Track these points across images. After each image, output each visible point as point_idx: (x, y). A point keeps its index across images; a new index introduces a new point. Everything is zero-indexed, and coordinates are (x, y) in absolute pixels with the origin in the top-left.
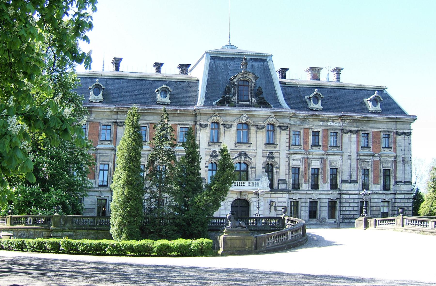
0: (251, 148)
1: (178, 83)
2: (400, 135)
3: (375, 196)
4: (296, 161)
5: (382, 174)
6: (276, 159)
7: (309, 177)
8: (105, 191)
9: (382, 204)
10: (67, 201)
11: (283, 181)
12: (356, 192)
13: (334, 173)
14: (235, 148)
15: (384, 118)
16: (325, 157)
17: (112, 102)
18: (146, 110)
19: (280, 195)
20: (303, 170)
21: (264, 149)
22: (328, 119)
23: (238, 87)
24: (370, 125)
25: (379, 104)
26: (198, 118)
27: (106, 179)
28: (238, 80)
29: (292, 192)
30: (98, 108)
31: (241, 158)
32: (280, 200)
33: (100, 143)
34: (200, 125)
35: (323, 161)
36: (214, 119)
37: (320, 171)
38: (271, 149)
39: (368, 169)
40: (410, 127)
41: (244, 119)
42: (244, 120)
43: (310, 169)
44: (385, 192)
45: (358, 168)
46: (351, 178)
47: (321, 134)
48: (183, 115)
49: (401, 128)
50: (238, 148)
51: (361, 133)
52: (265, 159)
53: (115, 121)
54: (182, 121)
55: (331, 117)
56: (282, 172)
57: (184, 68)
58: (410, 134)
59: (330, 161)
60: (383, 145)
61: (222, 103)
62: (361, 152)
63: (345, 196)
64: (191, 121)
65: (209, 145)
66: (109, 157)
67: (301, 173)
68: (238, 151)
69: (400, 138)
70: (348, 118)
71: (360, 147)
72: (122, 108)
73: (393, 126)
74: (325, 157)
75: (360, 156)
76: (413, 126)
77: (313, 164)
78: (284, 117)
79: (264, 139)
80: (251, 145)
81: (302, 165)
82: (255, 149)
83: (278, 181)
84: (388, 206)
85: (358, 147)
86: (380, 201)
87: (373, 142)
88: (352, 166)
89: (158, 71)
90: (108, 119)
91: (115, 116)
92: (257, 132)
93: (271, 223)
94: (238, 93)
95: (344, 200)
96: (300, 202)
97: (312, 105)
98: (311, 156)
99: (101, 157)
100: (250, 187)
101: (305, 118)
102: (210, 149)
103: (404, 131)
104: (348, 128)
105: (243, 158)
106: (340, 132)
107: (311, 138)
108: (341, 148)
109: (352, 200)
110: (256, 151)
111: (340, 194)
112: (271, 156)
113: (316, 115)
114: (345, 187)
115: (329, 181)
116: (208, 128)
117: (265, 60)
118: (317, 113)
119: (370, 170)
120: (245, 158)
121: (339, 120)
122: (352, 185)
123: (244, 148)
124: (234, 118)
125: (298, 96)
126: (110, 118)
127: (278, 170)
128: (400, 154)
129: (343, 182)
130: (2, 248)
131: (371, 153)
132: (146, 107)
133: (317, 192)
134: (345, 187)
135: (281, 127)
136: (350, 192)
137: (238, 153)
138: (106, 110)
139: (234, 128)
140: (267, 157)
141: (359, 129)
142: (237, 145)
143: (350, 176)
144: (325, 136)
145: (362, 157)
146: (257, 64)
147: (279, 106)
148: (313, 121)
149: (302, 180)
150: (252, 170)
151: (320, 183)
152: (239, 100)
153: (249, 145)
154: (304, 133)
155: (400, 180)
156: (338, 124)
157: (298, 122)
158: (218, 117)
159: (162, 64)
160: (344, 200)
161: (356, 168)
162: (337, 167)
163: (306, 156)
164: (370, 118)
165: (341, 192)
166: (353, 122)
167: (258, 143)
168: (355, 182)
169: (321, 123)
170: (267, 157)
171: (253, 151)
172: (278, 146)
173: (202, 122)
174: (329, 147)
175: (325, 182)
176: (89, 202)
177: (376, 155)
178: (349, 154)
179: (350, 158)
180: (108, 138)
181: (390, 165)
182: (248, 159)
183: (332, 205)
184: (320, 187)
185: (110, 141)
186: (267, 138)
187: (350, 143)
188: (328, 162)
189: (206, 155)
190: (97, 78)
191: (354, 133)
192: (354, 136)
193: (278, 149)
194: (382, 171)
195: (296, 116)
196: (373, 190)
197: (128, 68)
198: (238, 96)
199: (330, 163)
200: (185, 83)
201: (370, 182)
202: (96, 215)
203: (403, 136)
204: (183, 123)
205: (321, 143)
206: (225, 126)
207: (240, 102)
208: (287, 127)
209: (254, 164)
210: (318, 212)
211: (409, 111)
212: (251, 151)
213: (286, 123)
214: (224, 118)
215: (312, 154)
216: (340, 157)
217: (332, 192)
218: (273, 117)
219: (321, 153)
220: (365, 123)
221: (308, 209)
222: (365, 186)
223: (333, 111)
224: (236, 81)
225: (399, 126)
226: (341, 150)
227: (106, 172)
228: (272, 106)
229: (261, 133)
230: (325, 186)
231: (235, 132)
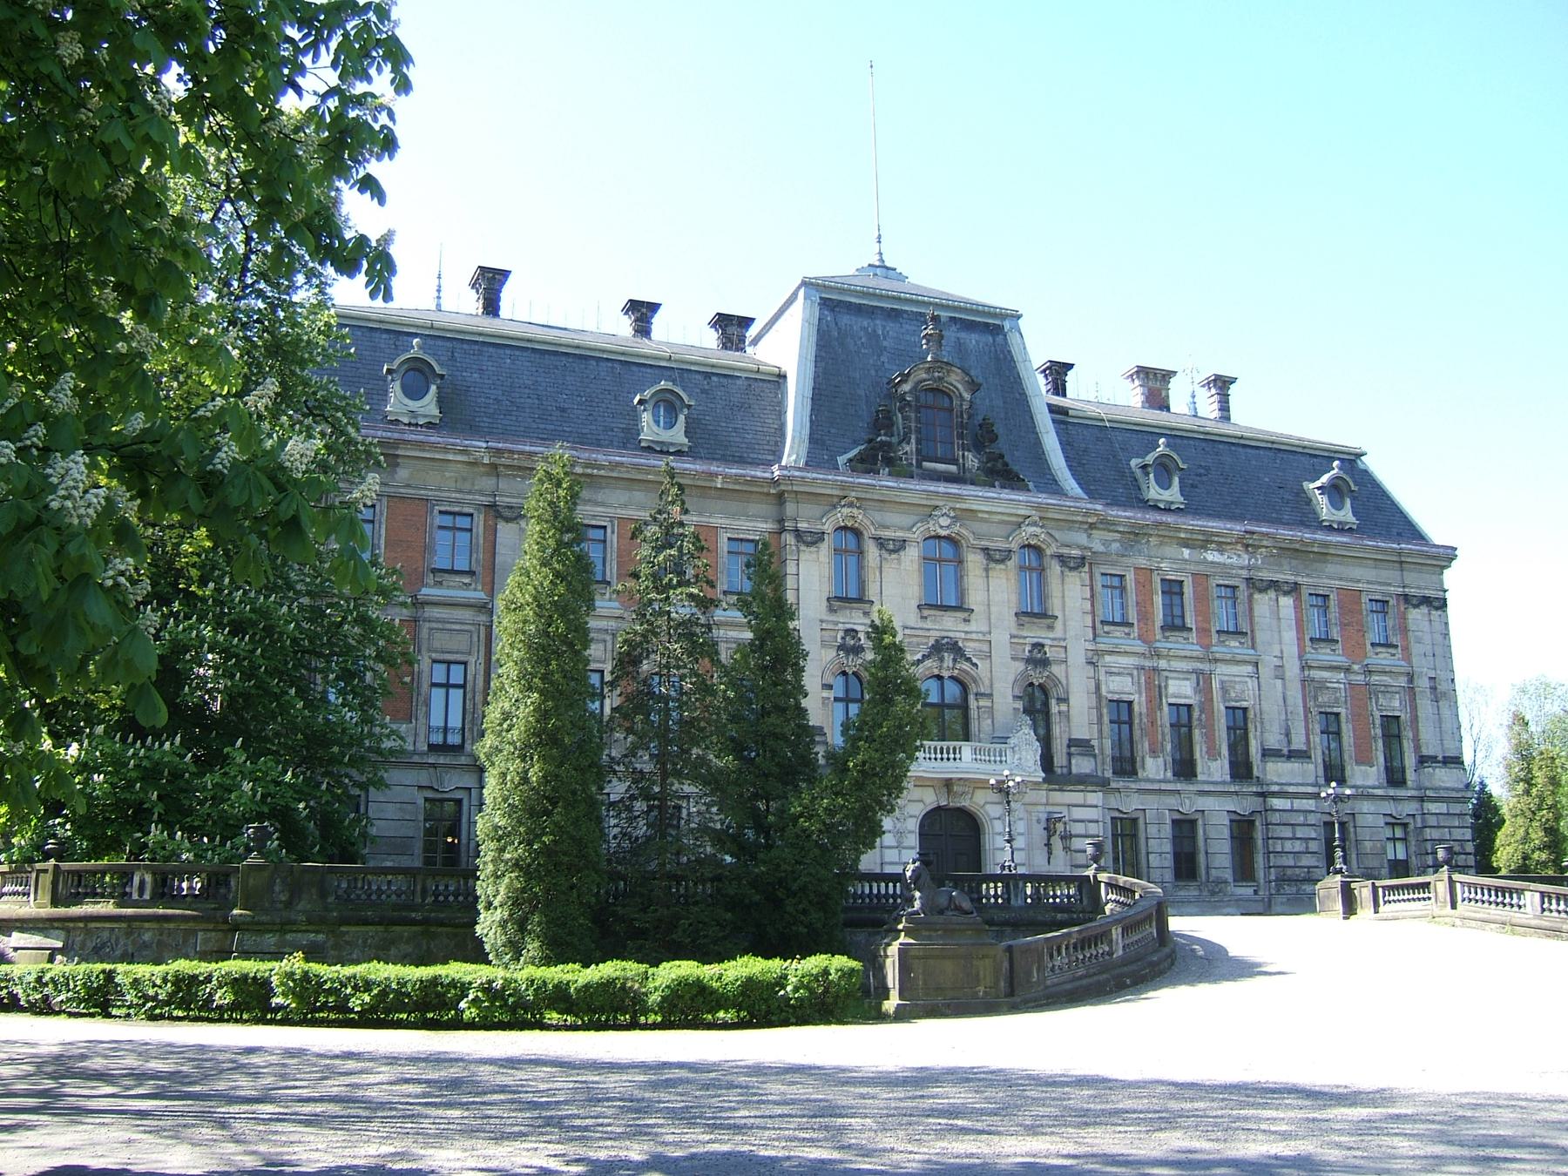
0: (973, 627)
1: (714, 379)
2: (1416, 606)
3: (1366, 806)
4: (1118, 678)
5: (1379, 732)
6: (1056, 670)
7: (1163, 734)
8: (454, 767)
9: (1388, 833)
10: (301, 806)
11: (1080, 746)
12: (1310, 790)
13: (1240, 721)
14: (921, 625)
15: (1364, 548)
16: (1206, 667)
17: (473, 430)
18: (600, 467)
19: (1076, 797)
20: (1144, 711)
21: (1015, 632)
22: (1205, 541)
23: (918, 410)
24: (1330, 568)
25: (1348, 502)
26: (790, 508)
27: (455, 721)
28: (914, 388)
29: (1113, 785)
30: (420, 445)
31: (942, 660)
32: (1078, 813)
33: (430, 579)
34: (798, 534)
35: (1203, 681)
36: (842, 515)
37: (1196, 714)
38: (1034, 633)
39: (1337, 715)
40: (1441, 582)
41: (945, 521)
42: (942, 526)
43: (1166, 708)
44: (1392, 792)
45: (1307, 711)
46: (1289, 742)
47: (1188, 590)
48: (738, 493)
49: (1418, 584)
50: (928, 624)
51: (1305, 592)
52: (1021, 666)
53: (486, 500)
54: (733, 516)
55: (1213, 534)
56: (1079, 716)
57: (732, 327)
58: (1442, 604)
59: (1222, 682)
60: (1373, 636)
61: (866, 463)
62: (1312, 655)
63: (1277, 803)
64: (765, 519)
65: (831, 610)
66: (467, 636)
67: (1136, 721)
68: (931, 633)
69: (1416, 616)
70: (1265, 543)
71: (1307, 638)
72: (512, 452)
73: (1391, 574)
74: (1206, 667)
75: (1310, 667)
76: (1450, 577)
77: (1171, 690)
78: (1070, 524)
79: (1014, 598)
80: (973, 616)
81: (1140, 693)
82: (985, 629)
83: (1069, 747)
84: (1404, 839)
85: (1300, 639)
86: (1381, 821)
87: (1343, 626)
88: (1290, 701)
89: (643, 329)
90: (460, 491)
91: (488, 483)
92: (987, 570)
93: (1055, 896)
94: (918, 431)
95: (1275, 818)
96: (1141, 822)
97: (1154, 492)
98: (1163, 664)
99: (438, 635)
100: (977, 765)
101: (1135, 535)
102: (836, 623)
103: (1427, 593)
104: (1266, 575)
105: (948, 658)
106: (1243, 586)
107: (1158, 599)
108: (1253, 638)
109: (1301, 819)
110: (987, 637)
111: (1263, 795)
112: (1038, 658)
113: (1167, 525)
114: (1277, 772)
115: (1225, 751)
116: (825, 549)
117: (997, 330)
118: (1169, 519)
119: (1343, 718)
120: (955, 660)
121: (1239, 547)
123: (949, 625)
124: (913, 519)
125: (1105, 452)
126: (467, 486)
127: (1063, 707)
128: (1422, 666)
129: (1267, 753)
130: (10, 1005)
131: (1340, 659)
132: (601, 458)
133: (1191, 788)
134: (1277, 772)
135: (1062, 559)
136: (1291, 789)
137: (932, 642)
138: (451, 457)
139: (912, 554)
140: (1028, 661)
141: (1300, 580)
142: (926, 613)
143: (1288, 734)
144: (1202, 598)
145: (1317, 674)
147: (1050, 484)
148: (1161, 543)
149: (1143, 746)
150: (981, 703)
151: (1197, 755)
152: (922, 456)
153: (965, 615)
154: (1137, 582)
155: (1431, 753)
156: (1234, 560)
157: (1115, 546)
158: (855, 511)
159: (654, 307)
160: (1275, 818)
161: (1301, 710)
162: (1244, 704)
163: (1148, 663)
164: (1325, 545)
165: (1265, 789)
166: (1279, 556)
167: (993, 609)
168: (1302, 755)
169: (1186, 552)
170: (1028, 661)
171: (980, 637)
172: (1059, 624)
173: (803, 526)
174: (1215, 637)
175: (1213, 754)
176: (391, 811)
177: (1356, 667)
178: (1277, 662)
180: (461, 564)
181: (1397, 704)
182: (966, 666)
184: (1199, 769)
185: (471, 573)
186: (1021, 594)
188: (1215, 685)
189: (824, 644)
190: (416, 335)
191: (1286, 593)
192: (1287, 602)
193: (1058, 633)
194: (1378, 722)
195: (1106, 524)
196: (1359, 783)
197: (524, 308)
198: (918, 442)
199: (1224, 690)
200: (739, 382)
201: (1346, 757)
202: (418, 863)
203: (1424, 609)
204: (736, 524)
205: (1190, 621)
206: (881, 543)
207: (926, 464)
208: (1083, 558)
209: (987, 683)
210: (1201, 858)
211: (1437, 533)
212: (974, 636)
213: (1079, 547)
214: (878, 517)
215: (1168, 657)
216: (1250, 668)
217: (1237, 788)
218: (1035, 524)
219: (1195, 654)
220: (1314, 561)
221: (1168, 847)
222: (1334, 772)
223: (1217, 516)
224: (910, 392)
225: (1410, 577)
226: (1253, 647)
227: (456, 695)
228: (1031, 485)
229: (1003, 575)
230: (1214, 769)
231: (916, 566)
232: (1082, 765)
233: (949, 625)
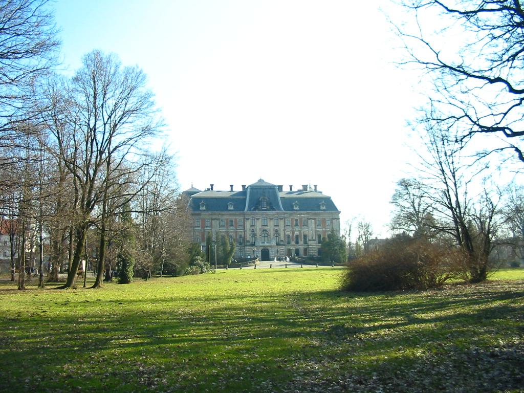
13: (305, 236)
22: (301, 214)
24: (321, 215)
35: (300, 232)
48: (240, 214)
58: (339, 219)
61: (255, 210)
97: (295, 208)
101: (291, 214)
112: (277, 231)
114: (310, 242)
122: (313, 242)
123: (265, 228)
125: (289, 204)
134: (310, 242)
139: (260, 220)
146: (271, 190)
147: (279, 209)
179: (312, 230)
183: (305, 250)
187: (312, 224)
192: (313, 221)
195: (287, 213)
205: (299, 224)
211: (339, 210)
232: (282, 243)
233: (265, 228)
